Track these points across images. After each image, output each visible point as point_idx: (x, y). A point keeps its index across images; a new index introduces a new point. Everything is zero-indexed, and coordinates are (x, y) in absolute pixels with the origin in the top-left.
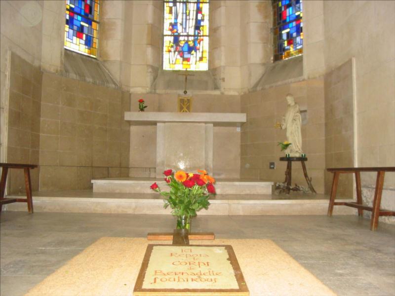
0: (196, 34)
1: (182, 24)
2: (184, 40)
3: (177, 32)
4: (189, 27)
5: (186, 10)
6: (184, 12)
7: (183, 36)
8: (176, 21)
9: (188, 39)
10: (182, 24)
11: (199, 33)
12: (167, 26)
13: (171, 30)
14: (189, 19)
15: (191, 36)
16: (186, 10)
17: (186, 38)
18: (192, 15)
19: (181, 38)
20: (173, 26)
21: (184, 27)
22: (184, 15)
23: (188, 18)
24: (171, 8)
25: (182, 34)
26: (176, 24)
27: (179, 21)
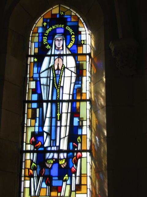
0: (71, 148)
1: (49, 134)
2: (52, 159)
3: (42, 145)
4: (60, 139)
5: (57, 113)
6: (54, 115)
7: (51, 152)
8: (41, 130)
9: (58, 156)
10: (49, 134)
11: (74, 147)
12: (28, 136)
13: (32, 143)
14: (61, 126)
15: (63, 151)
16: (57, 113)
17: (56, 156)
18: (65, 120)
19: (49, 156)
20: (37, 136)
21: (53, 138)
22: (54, 120)
23: (59, 124)
24: (34, 110)
25: (49, 149)
26: (41, 134)
27: (46, 129)
